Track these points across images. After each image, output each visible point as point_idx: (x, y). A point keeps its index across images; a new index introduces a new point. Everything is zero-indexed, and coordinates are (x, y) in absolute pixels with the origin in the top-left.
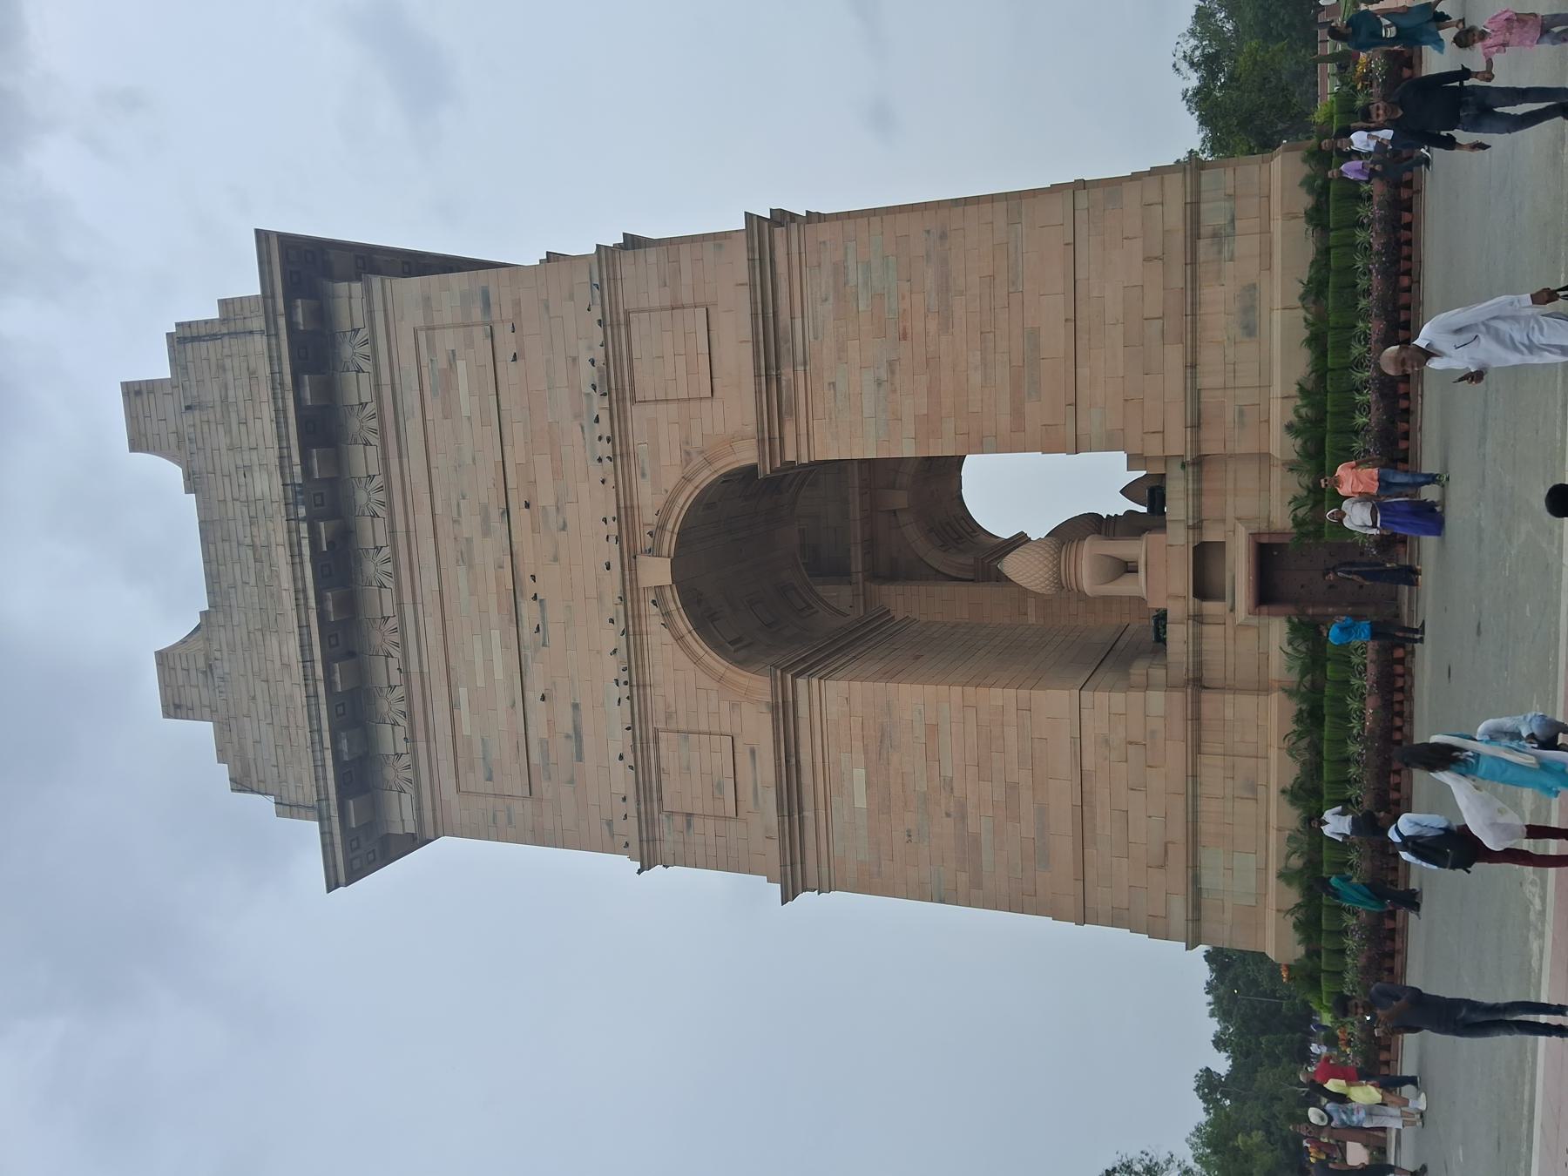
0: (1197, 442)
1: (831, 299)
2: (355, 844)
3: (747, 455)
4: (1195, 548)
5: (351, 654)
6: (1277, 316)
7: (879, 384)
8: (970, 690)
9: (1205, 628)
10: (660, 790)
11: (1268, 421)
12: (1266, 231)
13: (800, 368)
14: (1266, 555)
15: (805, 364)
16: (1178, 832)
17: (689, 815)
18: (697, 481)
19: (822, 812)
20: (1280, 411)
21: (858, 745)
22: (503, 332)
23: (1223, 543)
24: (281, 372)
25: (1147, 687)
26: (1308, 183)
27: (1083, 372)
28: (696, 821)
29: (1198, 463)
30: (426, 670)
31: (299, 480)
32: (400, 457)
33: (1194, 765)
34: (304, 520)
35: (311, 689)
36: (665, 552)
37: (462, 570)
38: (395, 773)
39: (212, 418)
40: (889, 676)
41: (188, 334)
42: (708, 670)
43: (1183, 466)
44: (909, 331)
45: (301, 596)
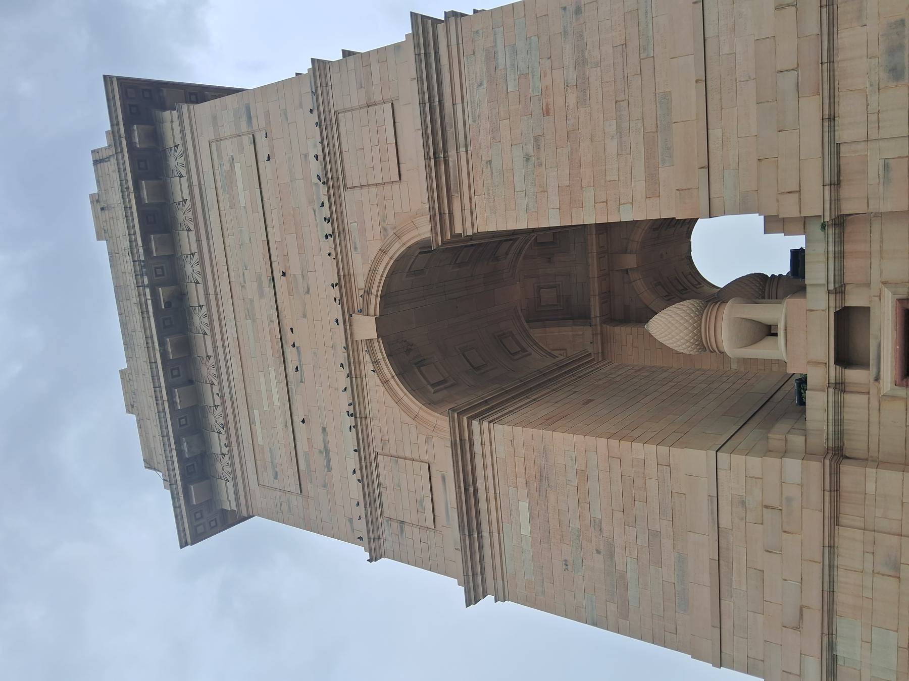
0: (836, 201)
1: (485, 84)
2: (198, 515)
3: (423, 231)
4: (837, 314)
5: (191, 382)
7: (528, 160)
8: (614, 443)
10: (380, 500)
13: (463, 150)
15: (466, 145)
16: (814, 598)
17: (402, 522)
19: (495, 535)
21: (521, 481)
22: (260, 138)
23: (867, 309)
24: (126, 180)
27: (715, 133)
28: (407, 528)
29: (840, 222)
30: (234, 396)
31: (142, 258)
33: (832, 536)
34: (147, 286)
35: (160, 406)
36: (372, 312)
37: (249, 322)
38: (222, 467)
40: (549, 423)
42: (406, 409)
43: (823, 227)
44: (551, 107)
45: (150, 341)
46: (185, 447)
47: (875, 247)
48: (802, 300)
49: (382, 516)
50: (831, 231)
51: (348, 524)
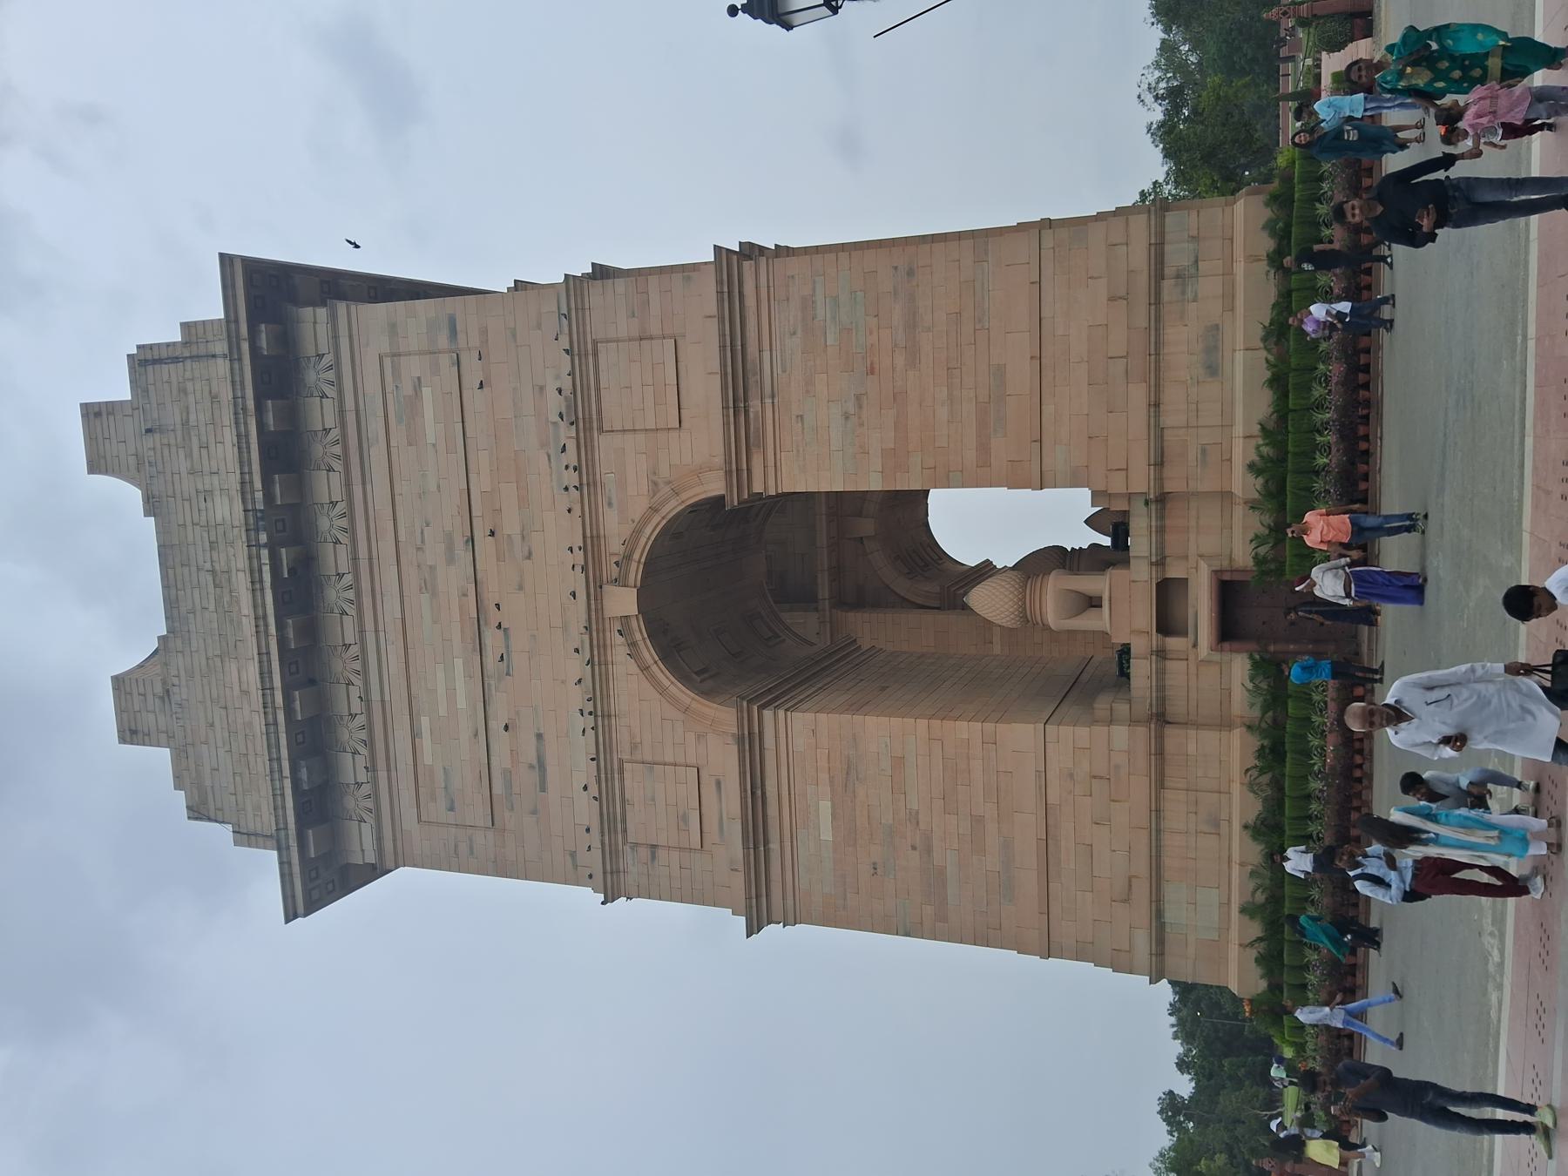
0: (1160, 480)
2: (313, 874)
3: (714, 486)
5: (312, 682)
6: (1239, 356)
8: (936, 723)
9: (1168, 663)
10: (624, 821)
11: (1230, 460)
12: (1228, 273)
13: (768, 401)
14: (1228, 592)
15: (773, 397)
16: (1142, 867)
17: (654, 847)
18: (664, 511)
19: (787, 844)
20: (1242, 452)
21: (824, 777)
22: (469, 360)
24: (243, 397)
25: (1111, 722)
26: (1270, 227)
27: (1048, 409)
28: (661, 853)
29: (1162, 499)
30: (387, 698)
31: (260, 506)
32: (364, 483)
34: (265, 546)
37: (425, 597)
38: (355, 803)
39: (172, 442)
40: (856, 707)
41: (149, 357)
42: (674, 701)
43: (1147, 503)
45: (261, 623)
46: (304, 774)
47: (1193, 523)
48: (1125, 572)
49: (625, 842)
50: (1153, 507)
51: (569, 858)
